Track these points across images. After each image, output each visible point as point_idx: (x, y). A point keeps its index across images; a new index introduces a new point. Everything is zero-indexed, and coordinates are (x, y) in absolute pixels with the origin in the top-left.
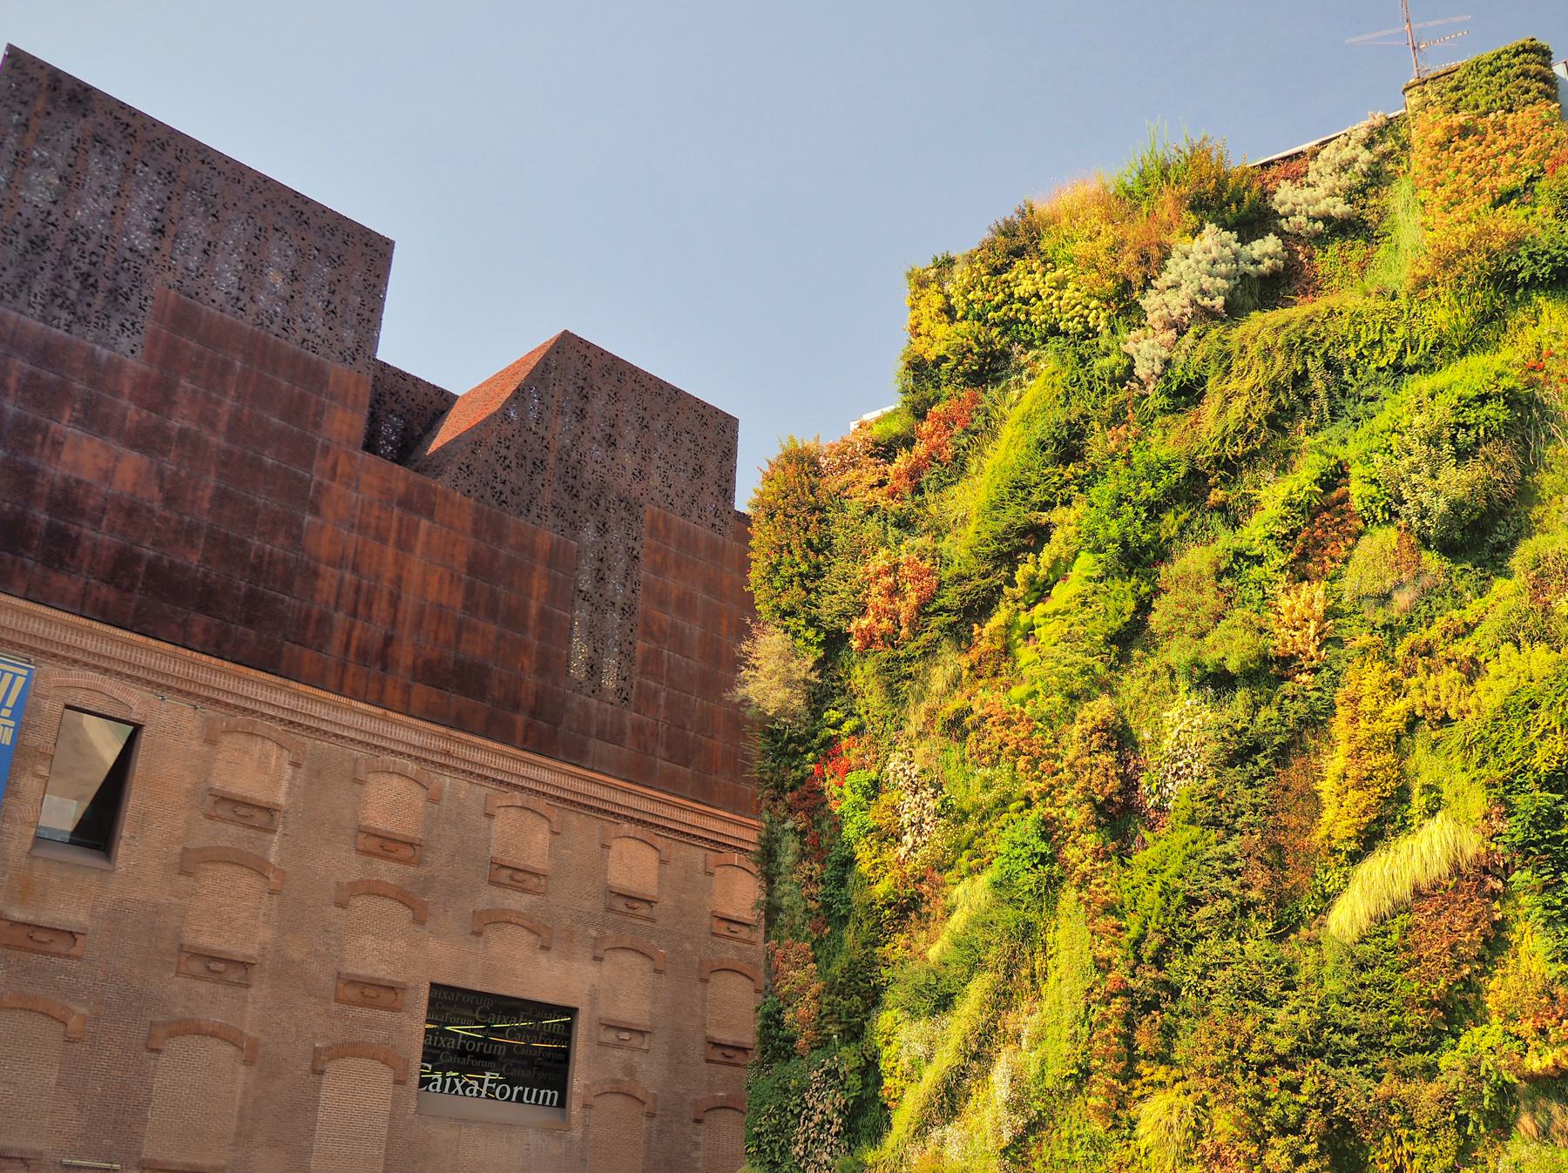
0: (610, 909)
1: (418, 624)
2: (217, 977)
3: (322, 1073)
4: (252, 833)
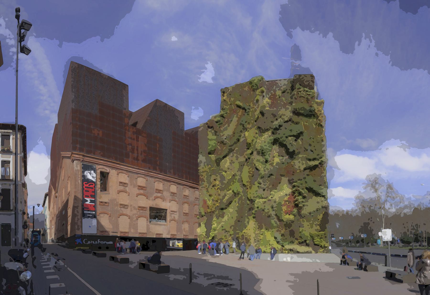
0: (171, 195)
1: (141, 154)
2: (124, 207)
3: (138, 219)
4: (124, 187)
